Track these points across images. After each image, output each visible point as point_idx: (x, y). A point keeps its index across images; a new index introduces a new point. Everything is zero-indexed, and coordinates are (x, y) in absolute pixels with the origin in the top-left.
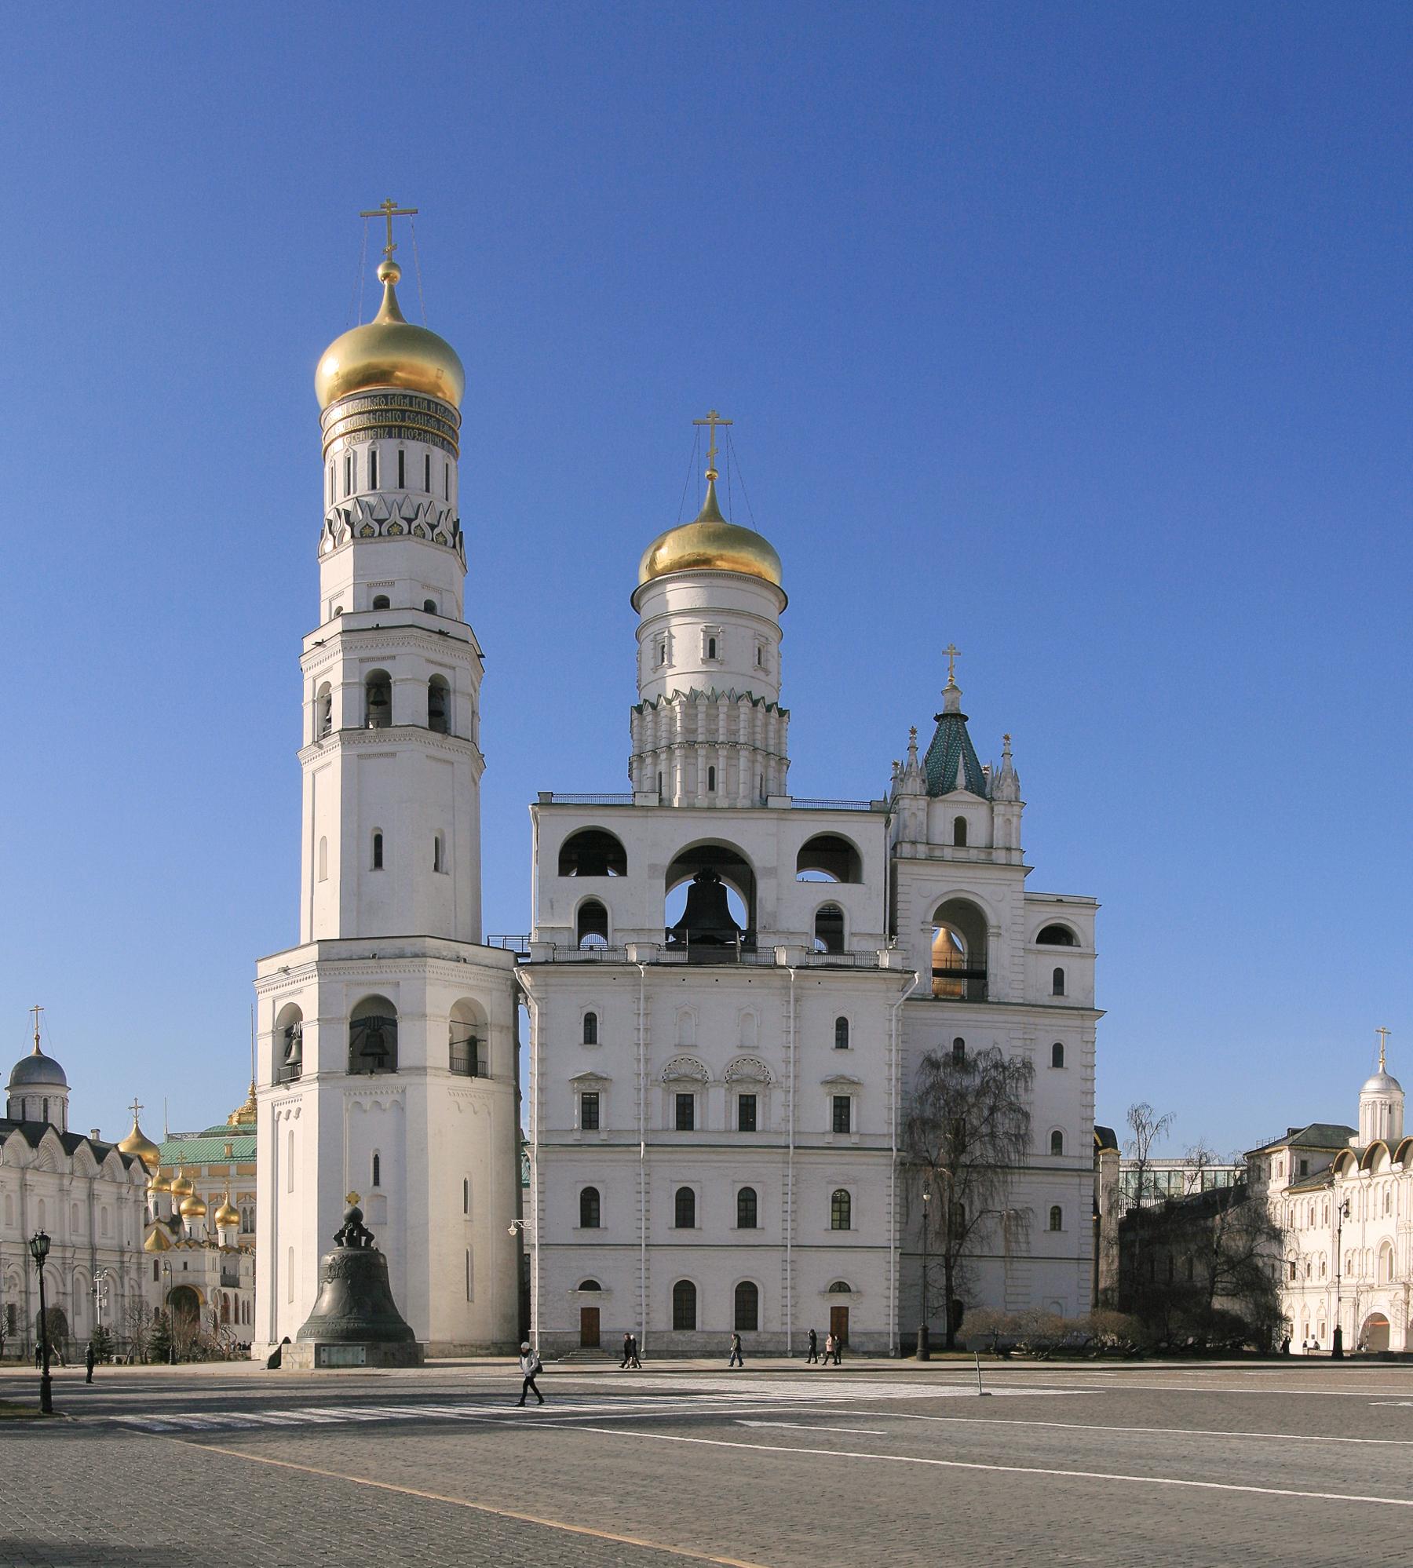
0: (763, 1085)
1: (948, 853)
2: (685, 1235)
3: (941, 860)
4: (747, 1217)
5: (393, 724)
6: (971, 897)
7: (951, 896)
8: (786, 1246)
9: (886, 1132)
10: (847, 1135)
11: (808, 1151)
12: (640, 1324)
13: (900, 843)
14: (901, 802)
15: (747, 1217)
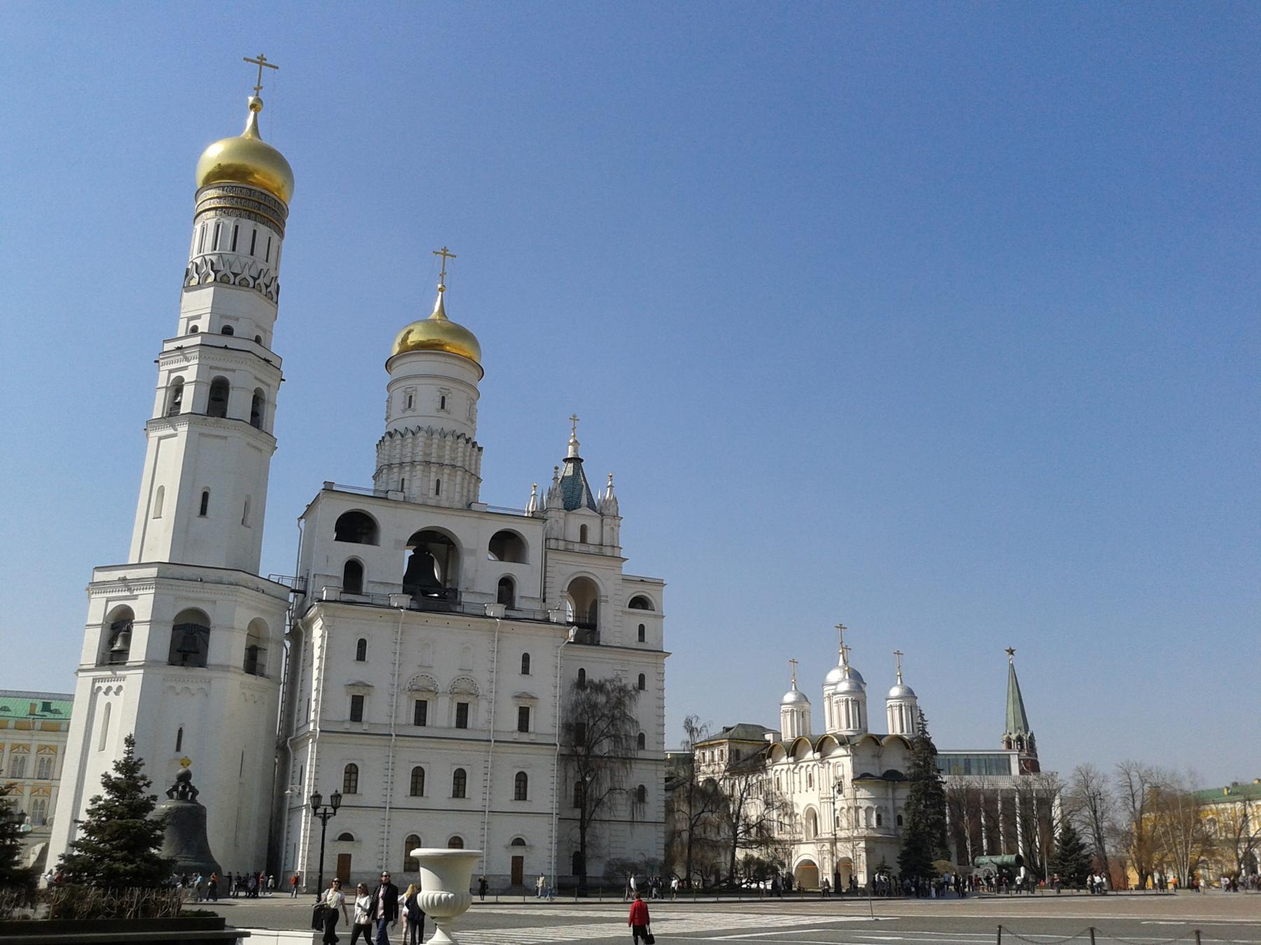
0: (474, 696)
1: (577, 547)
2: (417, 802)
3: (572, 551)
4: (459, 788)
5: (227, 417)
6: (592, 577)
7: (579, 575)
8: (485, 812)
9: (552, 732)
10: (526, 733)
11: (503, 744)
12: (381, 867)
13: (549, 539)
14: (549, 513)
15: (459, 788)
